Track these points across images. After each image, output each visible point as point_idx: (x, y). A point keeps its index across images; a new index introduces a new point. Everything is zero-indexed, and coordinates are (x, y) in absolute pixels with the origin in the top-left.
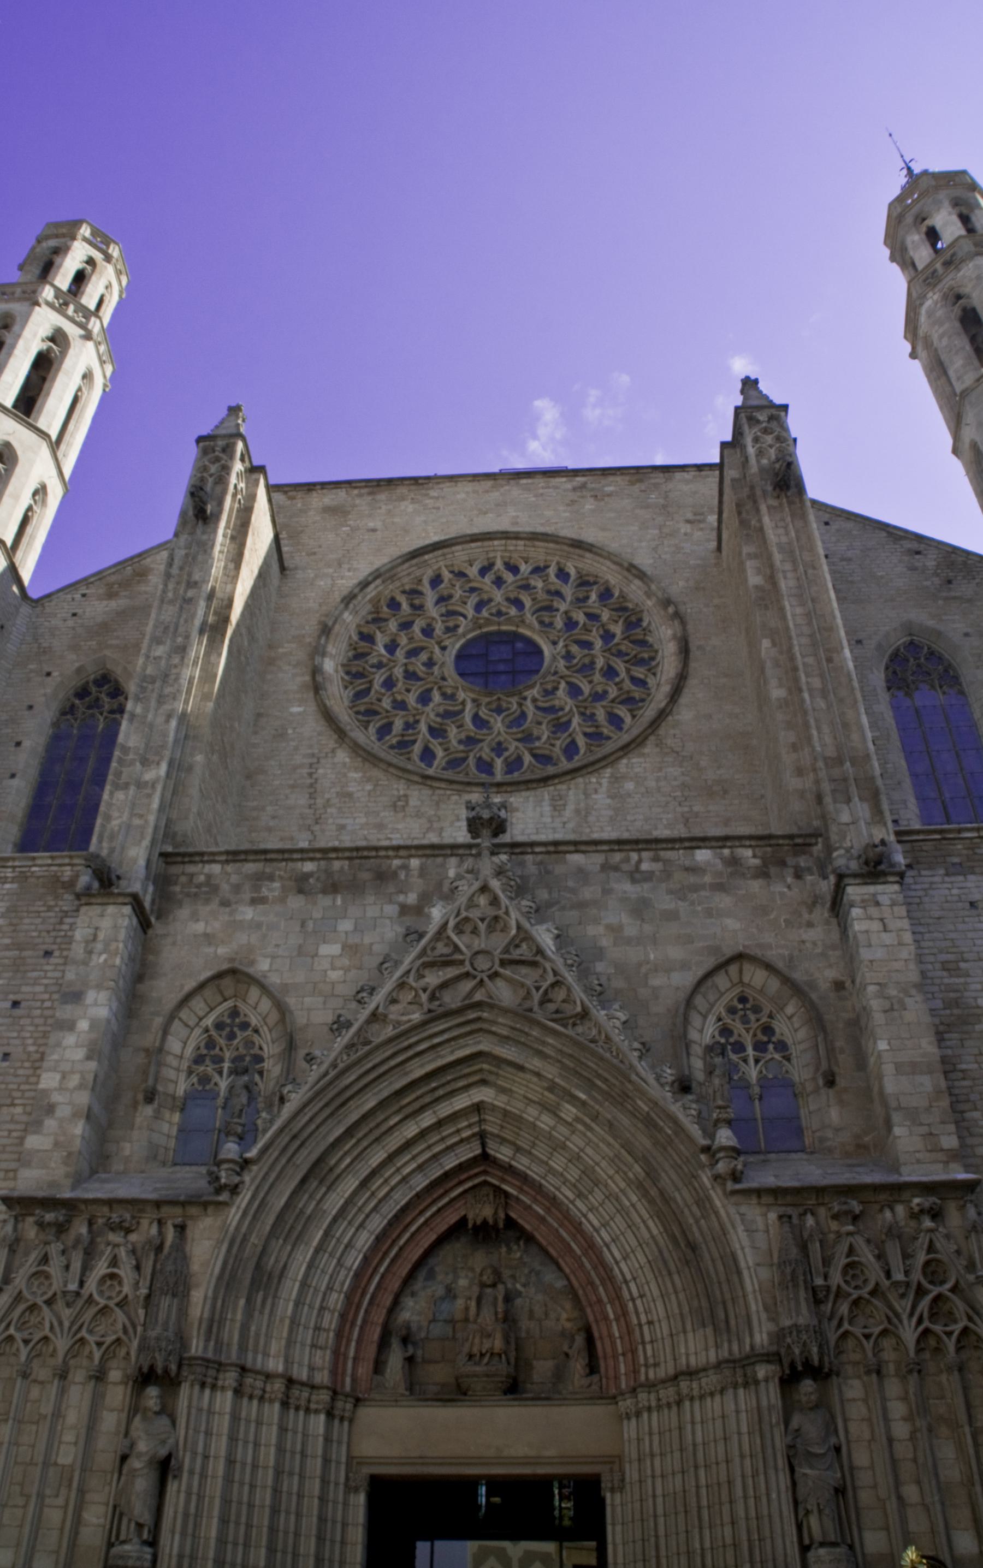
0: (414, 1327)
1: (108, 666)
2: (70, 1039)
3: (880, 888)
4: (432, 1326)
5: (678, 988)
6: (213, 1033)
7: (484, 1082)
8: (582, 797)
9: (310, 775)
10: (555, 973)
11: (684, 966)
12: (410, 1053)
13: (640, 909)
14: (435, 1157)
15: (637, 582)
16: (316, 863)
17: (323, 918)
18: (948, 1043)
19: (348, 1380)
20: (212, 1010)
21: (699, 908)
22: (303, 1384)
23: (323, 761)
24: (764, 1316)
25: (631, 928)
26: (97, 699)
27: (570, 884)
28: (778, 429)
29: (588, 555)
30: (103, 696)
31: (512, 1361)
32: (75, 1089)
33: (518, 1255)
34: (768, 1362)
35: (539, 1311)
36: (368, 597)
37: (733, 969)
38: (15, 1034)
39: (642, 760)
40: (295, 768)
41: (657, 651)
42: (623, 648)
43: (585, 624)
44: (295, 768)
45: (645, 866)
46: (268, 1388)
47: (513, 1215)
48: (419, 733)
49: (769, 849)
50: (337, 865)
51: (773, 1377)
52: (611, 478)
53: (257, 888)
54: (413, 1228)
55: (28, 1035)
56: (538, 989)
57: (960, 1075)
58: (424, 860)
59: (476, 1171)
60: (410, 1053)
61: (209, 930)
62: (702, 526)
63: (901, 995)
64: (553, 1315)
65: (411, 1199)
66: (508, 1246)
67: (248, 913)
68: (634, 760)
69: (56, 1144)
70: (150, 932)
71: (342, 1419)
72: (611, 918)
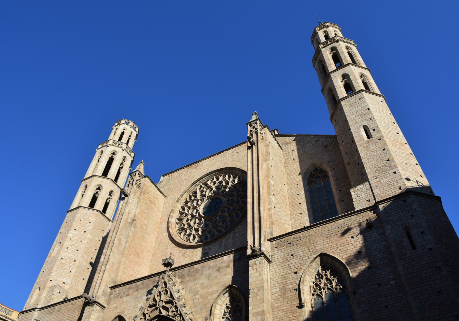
8: (226, 241)
9: (166, 251)
10: (176, 303)
11: (217, 291)
16: (141, 281)
18: (279, 302)
21: (222, 274)
29: (234, 171)
45: (211, 265)
48: (191, 234)
52: (242, 146)
53: (128, 292)
56: (171, 308)
57: (281, 311)
63: (258, 291)
67: (125, 299)
68: (239, 227)
72: (201, 281)
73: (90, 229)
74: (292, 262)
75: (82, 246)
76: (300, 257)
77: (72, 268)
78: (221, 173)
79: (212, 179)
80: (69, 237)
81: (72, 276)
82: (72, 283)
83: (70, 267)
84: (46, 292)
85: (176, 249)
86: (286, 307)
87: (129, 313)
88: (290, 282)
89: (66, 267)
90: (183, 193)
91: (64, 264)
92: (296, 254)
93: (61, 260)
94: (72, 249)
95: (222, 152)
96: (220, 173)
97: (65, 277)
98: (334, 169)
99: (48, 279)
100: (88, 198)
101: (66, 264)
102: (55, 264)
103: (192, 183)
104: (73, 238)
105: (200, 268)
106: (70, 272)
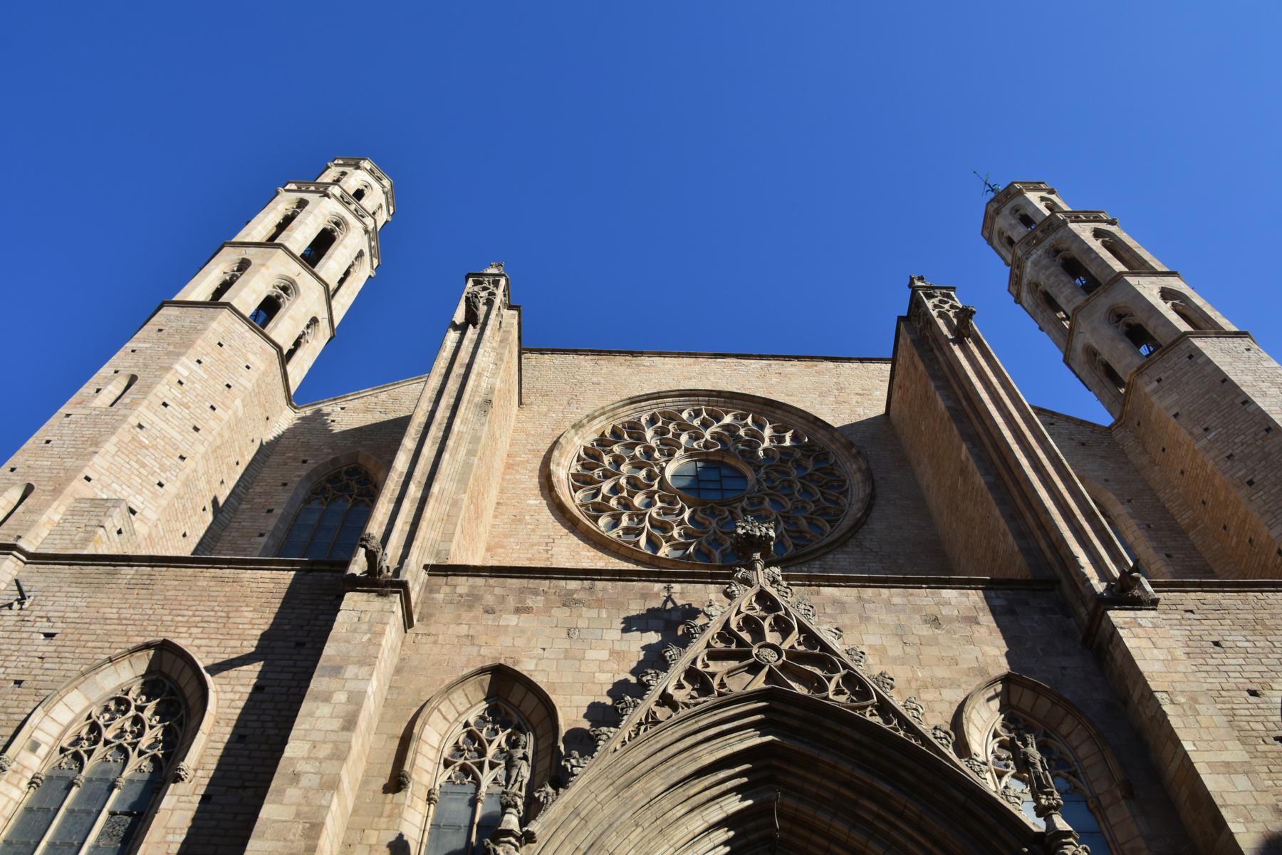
1: (360, 461)
2: (324, 710)
3: (1139, 613)
5: (951, 703)
6: (474, 728)
9: (547, 551)
10: (845, 666)
12: (700, 736)
13: (901, 634)
15: (821, 431)
16: (579, 582)
17: (588, 628)
20: (472, 706)
21: (957, 636)
23: (556, 541)
25: (895, 650)
26: (348, 485)
27: (828, 611)
28: (951, 302)
29: (778, 411)
30: (353, 483)
32: (326, 758)
36: (594, 428)
38: (255, 718)
39: (846, 556)
40: (533, 545)
41: (844, 481)
42: (815, 477)
43: (781, 458)
44: (533, 545)
45: (896, 600)
48: (643, 528)
49: (1009, 592)
50: (599, 584)
52: (791, 363)
55: (269, 718)
58: (684, 585)
60: (700, 736)
61: (470, 633)
62: (870, 397)
63: (1191, 702)
67: (513, 620)
68: (838, 556)
69: (298, 815)
73: (245, 388)
74: (1226, 661)
75: (212, 424)
76: (1249, 656)
77: (168, 473)
78: (731, 406)
79: (694, 410)
80: (177, 372)
81: (164, 503)
82: (156, 526)
83: (163, 468)
84: (62, 509)
85: (589, 554)
86: (1270, 783)
87: (543, 670)
88: (1247, 712)
89: (148, 461)
90: (596, 414)
91: (146, 447)
92: (1228, 644)
93: (138, 429)
94: (180, 417)
95: (724, 356)
96: (725, 402)
97: (140, 492)
98: (1129, 501)
99: (78, 469)
100: (255, 296)
101: (150, 449)
102: (113, 433)
103: (630, 398)
104: (189, 384)
105: (845, 599)
106: (160, 485)
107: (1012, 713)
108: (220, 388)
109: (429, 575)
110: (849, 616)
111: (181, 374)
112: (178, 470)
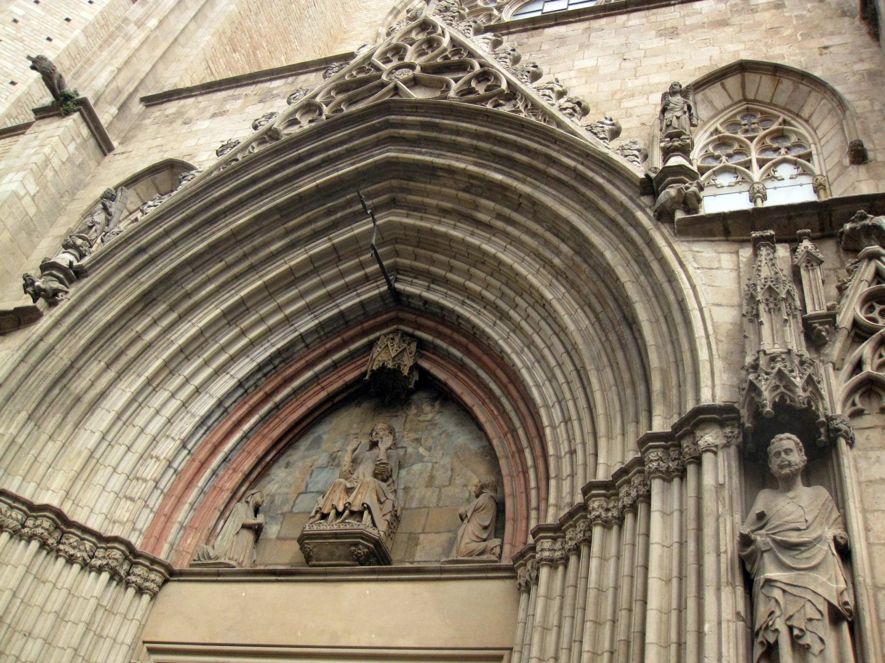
0: (278, 500)
4: (301, 497)
7: (393, 204)
14: (330, 296)
19: (166, 547)
22: (85, 530)
24: (719, 365)
31: (382, 526)
33: (430, 416)
34: (722, 424)
35: (441, 477)
37: (732, 82)
46: (30, 523)
47: (426, 365)
51: (726, 446)
54: (296, 383)
59: (384, 317)
64: (458, 481)
65: (292, 344)
66: (418, 407)
67: (206, 124)
70: (110, 156)
71: (140, 591)
94: (13, 49)
104: (24, 21)
107: (748, 109)
108: (58, 22)
109: (147, 106)
110: (568, 47)
111: (16, 14)
112: (8, 94)
